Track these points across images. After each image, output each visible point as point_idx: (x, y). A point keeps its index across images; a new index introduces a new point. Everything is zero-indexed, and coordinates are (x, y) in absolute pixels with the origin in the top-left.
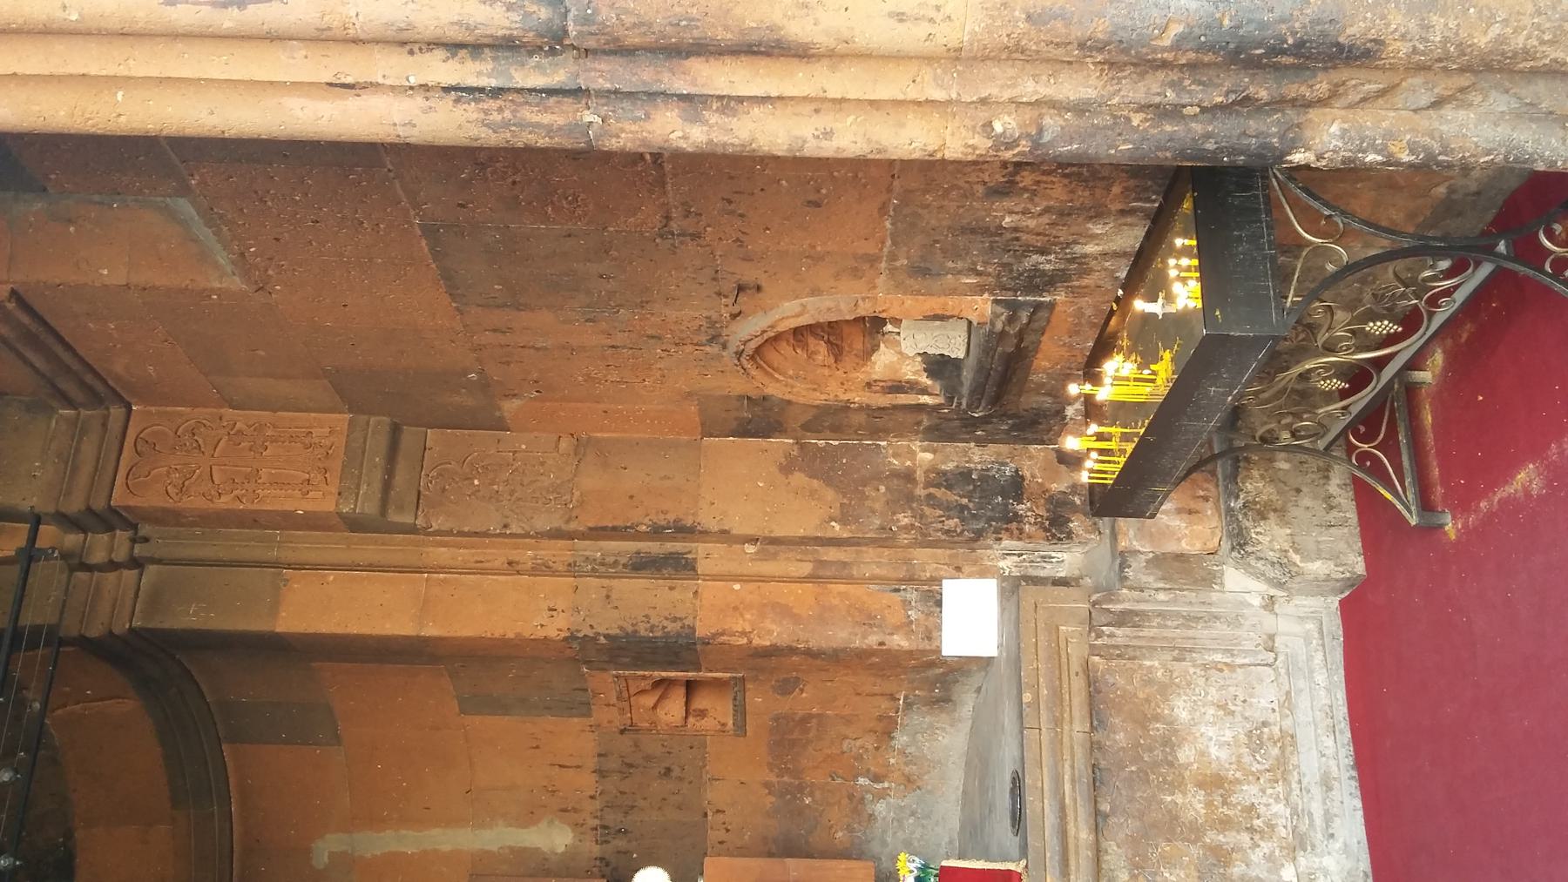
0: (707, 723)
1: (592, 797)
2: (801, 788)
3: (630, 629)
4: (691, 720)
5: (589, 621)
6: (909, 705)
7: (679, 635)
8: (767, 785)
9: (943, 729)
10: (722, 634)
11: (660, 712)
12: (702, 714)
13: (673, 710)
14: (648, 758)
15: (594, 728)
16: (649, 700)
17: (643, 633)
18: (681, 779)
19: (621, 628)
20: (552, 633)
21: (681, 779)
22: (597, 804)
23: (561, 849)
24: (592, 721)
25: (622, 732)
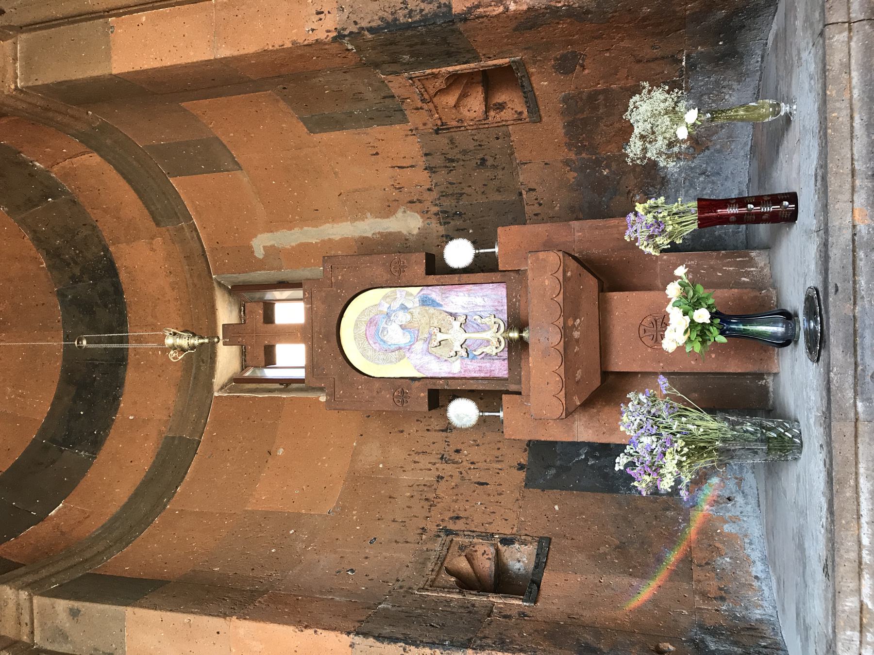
0: (507, 115)
1: (429, 190)
2: (598, 163)
3: (390, 18)
4: (492, 113)
5: (353, 17)
6: (691, 66)
7: (436, 15)
8: (567, 163)
9: (730, 87)
10: (478, 6)
11: (464, 112)
12: (501, 107)
13: (475, 104)
14: (465, 152)
15: (414, 131)
16: (451, 99)
17: (402, 20)
18: (494, 167)
19: (382, 19)
20: (321, 35)
21: (494, 167)
22: (435, 194)
23: (415, 232)
24: (410, 125)
25: (437, 132)
